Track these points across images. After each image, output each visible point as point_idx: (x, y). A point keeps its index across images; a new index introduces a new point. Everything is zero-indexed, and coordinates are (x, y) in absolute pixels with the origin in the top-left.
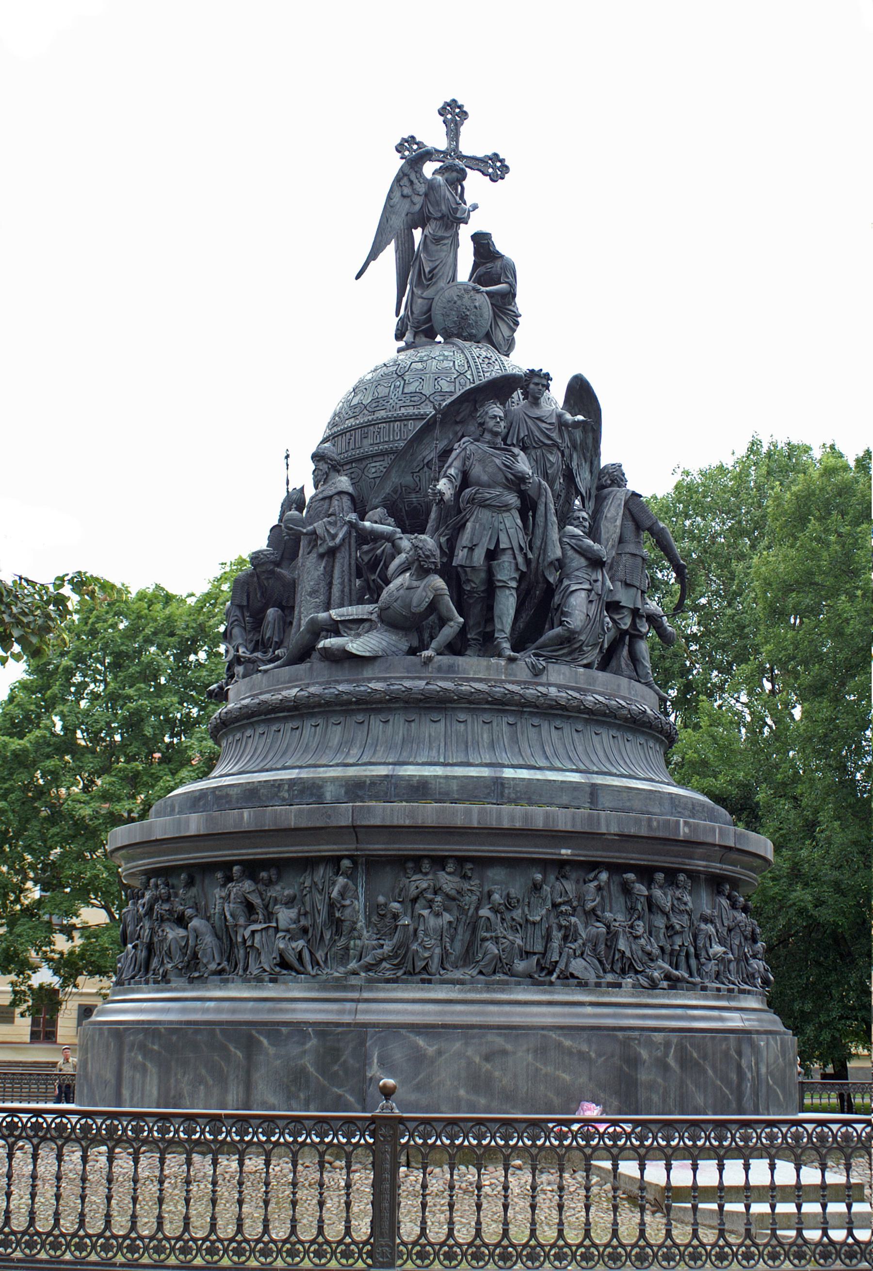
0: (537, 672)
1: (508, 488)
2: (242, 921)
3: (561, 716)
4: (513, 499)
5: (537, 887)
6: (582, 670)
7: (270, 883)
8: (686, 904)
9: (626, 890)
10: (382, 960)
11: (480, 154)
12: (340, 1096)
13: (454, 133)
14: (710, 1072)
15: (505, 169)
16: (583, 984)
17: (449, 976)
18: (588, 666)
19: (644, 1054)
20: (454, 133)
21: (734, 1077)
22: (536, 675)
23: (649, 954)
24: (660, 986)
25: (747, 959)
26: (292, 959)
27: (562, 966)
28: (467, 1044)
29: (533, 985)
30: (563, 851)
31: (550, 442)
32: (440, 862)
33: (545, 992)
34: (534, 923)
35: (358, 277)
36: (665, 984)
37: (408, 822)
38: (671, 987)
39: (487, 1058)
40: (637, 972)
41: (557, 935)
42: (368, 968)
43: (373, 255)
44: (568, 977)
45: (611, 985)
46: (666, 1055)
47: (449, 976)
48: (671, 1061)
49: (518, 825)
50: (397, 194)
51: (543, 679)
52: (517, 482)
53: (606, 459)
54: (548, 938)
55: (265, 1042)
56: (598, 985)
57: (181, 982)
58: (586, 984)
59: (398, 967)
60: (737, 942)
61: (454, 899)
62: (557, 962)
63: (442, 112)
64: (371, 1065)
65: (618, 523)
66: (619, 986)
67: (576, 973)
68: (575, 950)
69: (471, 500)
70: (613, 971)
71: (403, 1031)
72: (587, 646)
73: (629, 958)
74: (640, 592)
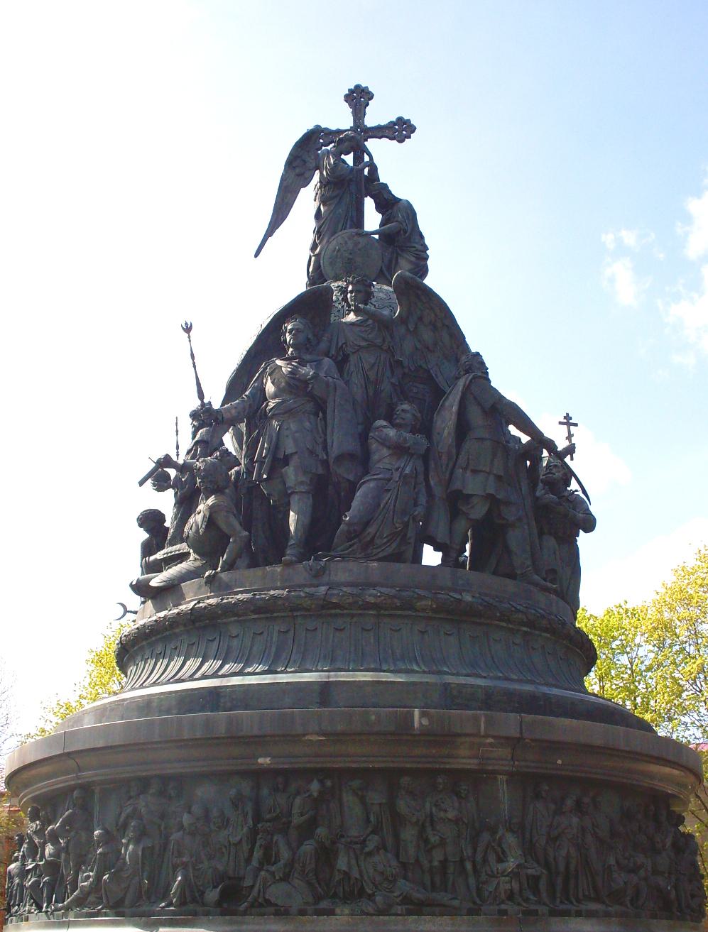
3: (342, 615)
6: (375, 564)
11: (384, 122)
13: (359, 112)
15: (412, 129)
20: (359, 112)
24: (393, 911)
27: (255, 892)
30: (260, 760)
35: (257, 255)
36: (399, 909)
38: (409, 913)
45: (320, 913)
51: (325, 579)
56: (302, 913)
65: (455, 409)
67: (273, 900)
68: (273, 874)
73: (356, 879)
74: (491, 478)
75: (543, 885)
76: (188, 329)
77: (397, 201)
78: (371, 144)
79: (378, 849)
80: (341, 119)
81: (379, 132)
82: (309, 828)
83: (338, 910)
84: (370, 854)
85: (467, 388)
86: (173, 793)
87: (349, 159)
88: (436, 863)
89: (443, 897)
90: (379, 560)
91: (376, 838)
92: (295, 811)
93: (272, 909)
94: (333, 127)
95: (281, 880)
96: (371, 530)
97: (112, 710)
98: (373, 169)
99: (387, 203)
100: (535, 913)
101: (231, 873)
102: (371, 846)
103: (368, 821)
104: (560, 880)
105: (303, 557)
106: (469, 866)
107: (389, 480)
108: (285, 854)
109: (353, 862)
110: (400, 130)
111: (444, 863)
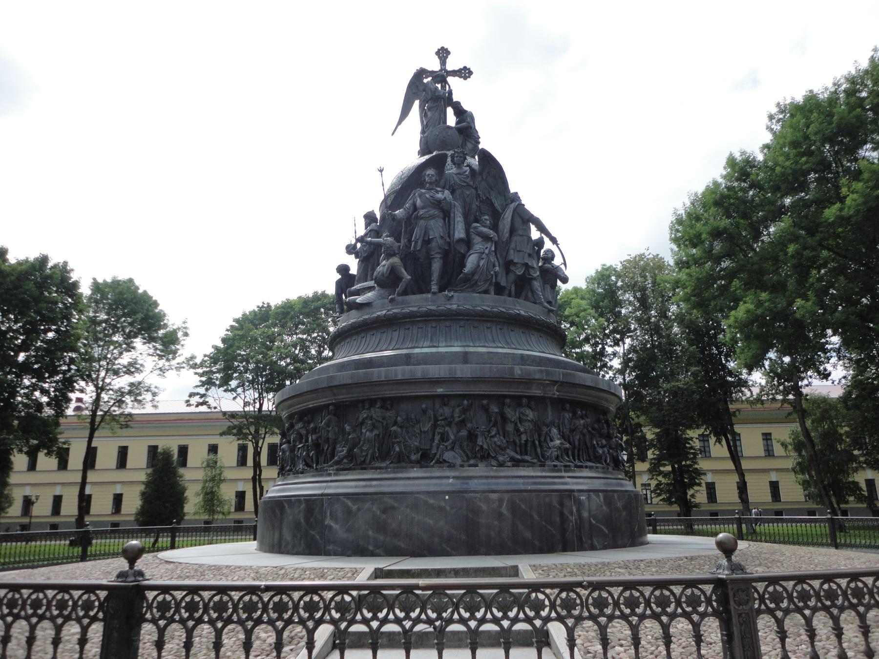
1: (435, 208)
3: (463, 320)
4: (436, 212)
6: (478, 294)
7: (309, 423)
8: (527, 416)
10: (343, 459)
11: (457, 68)
12: (313, 535)
13: (443, 62)
14: (536, 517)
15: (471, 73)
16: (451, 466)
18: (486, 292)
19: (484, 507)
20: (443, 62)
21: (558, 519)
23: (499, 446)
25: (595, 448)
26: (309, 461)
27: (438, 456)
28: (373, 504)
32: (372, 402)
33: (426, 472)
34: (425, 432)
35: (393, 134)
36: (509, 464)
38: (513, 466)
39: (384, 511)
40: (493, 458)
41: (437, 437)
42: (338, 463)
43: (400, 123)
44: (442, 462)
45: (470, 466)
46: (500, 506)
47: (377, 465)
48: (504, 510)
49: (407, 377)
53: (512, 191)
54: (433, 440)
55: (286, 506)
56: (462, 466)
59: (351, 461)
60: (578, 437)
61: (379, 422)
62: (436, 454)
63: (438, 53)
64: (326, 517)
66: (476, 466)
67: (447, 459)
70: (475, 457)
71: (341, 497)
72: (480, 282)
75: (570, 453)
76: (381, 171)
77: (465, 112)
78: (450, 79)
79: (496, 434)
80: (434, 65)
81: (454, 73)
82: (463, 422)
83: (479, 465)
84: (493, 437)
85: (515, 210)
86: (389, 407)
87: (439, 86)
88: (523, 442)
89: (527, 458)
90: (480, 293)
91: (495, 429)
92: (456, 415)
93: (447, 464)
94: (430, 69)
95: (450, 450)
96: (476, 277)
97: (348, 365)
98: (450, 93)
99: (460, 112)
100: (569, 466)
101: (423, 447)
102: (493, 433)
103: (490, 421)
104: (576, 451)
105: (441, 289)
106: (537, 443)
107: (483, 253)
108: (452, 437)
109: (484, 440)
110: (465, 73)
111: (526, 441)
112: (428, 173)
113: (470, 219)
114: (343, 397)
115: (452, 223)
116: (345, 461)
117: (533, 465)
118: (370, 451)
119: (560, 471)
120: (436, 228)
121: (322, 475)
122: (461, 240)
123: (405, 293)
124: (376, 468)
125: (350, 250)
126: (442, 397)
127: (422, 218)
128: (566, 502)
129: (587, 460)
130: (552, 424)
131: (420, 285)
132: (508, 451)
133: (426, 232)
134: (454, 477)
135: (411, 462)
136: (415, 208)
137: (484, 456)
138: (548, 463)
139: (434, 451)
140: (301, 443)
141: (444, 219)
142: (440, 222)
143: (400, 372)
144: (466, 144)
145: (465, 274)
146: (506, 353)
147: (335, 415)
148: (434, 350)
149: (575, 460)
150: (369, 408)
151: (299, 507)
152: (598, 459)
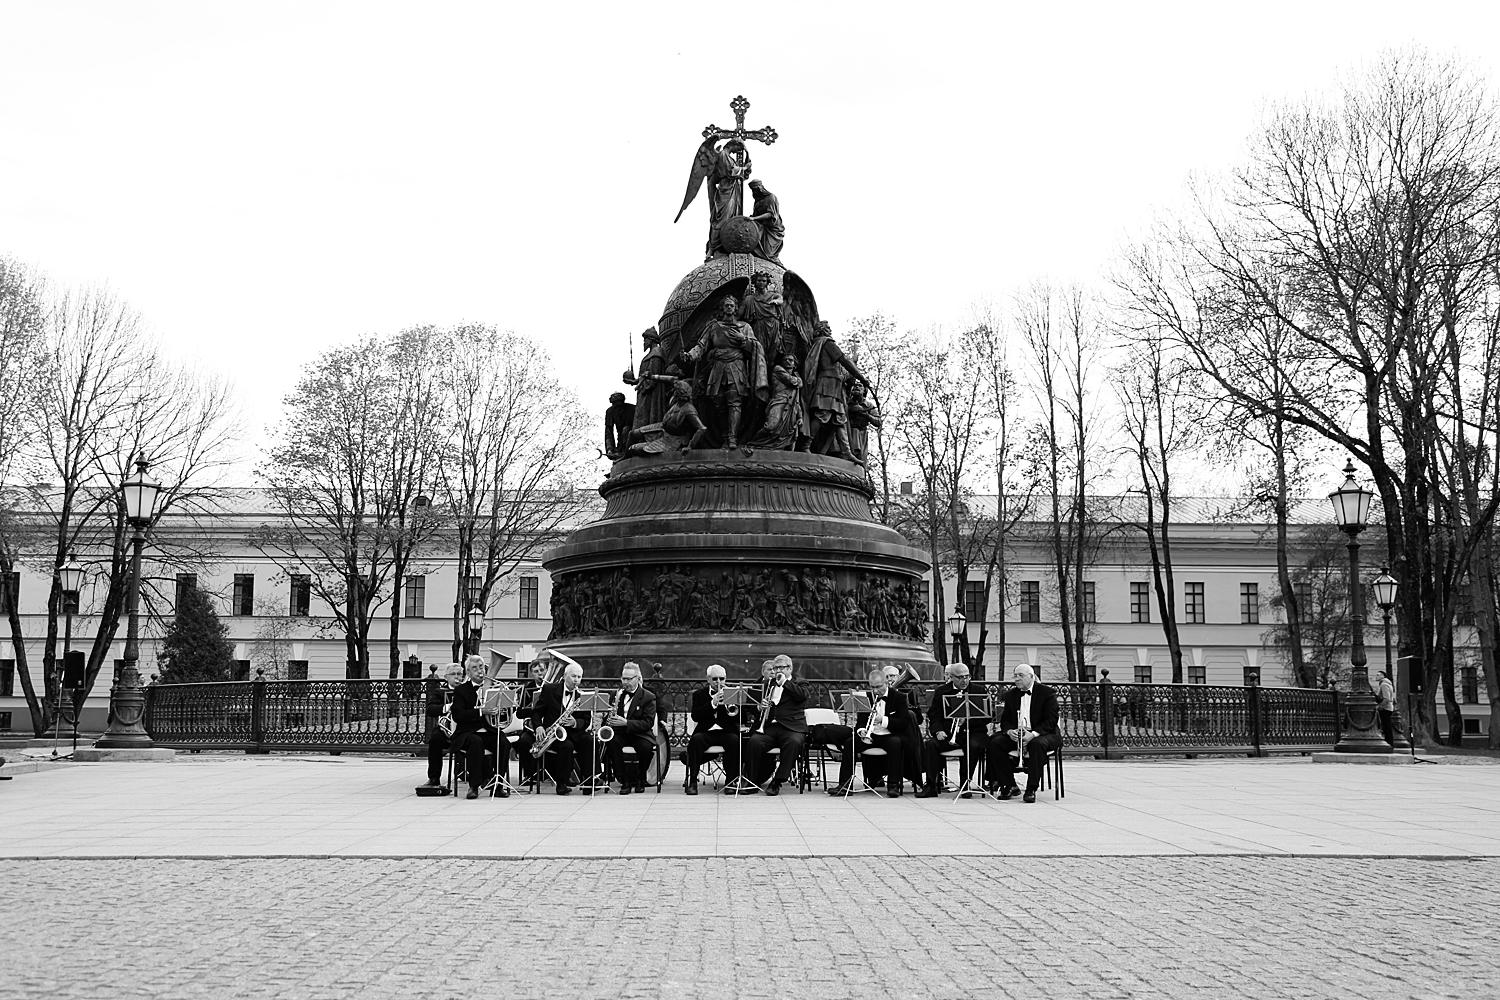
0: (749, 455)
1: (734, 348)
2: (583, 604)
4: (736, 354)
5: (725, 579)
7: (595, 582)
8: (825, 585)
9: (784, 578)
13: (740, 119)
15: (775, 135)
16: (750, 632)
17: (677, 629)
18: (788, 448)
20: (740, 119)
22: (748, 457)
23: (796, 614)
29: (721, 633)
31: (768, 315)
32: (671, 567)
37: (650, 546)
38: (809, 634)
41: (737, 605)
42: (633, 626)
43: (685, 206)
44: (741, 629)
47: (677, 629)
50: (698, 165)
52: (738, 344)
54: (732, 607)
56: (760, 632)
57: (559, 638)
58: (753, 632)
60: (875, 607)
61: (679, 587)
63: (733, 105)
65: (817, 359)
69: (713, 356)
70: (773, 625)
71: (644, 659)
75: (866, 622)
78: (749, 144)
80: (730, 124)
81: (756, 135)
84: (791, 605)
87: (734, 156)
89: (823, 626)
91: (793, 598)
102: (791, 602)
103: (789, 589)
110: (767, 136)
111: (823, 610)
112: (726, 303)
113: (775, 359)
114: (640, 560)
115: (753, 367)
116: (643, 624)
117: (827, 633)
118: (670, 615)
119: (854, 639)
120: (736, 372)
121: (618, 638)
122: (763, 388)
123: (698, 446)
124: (672, 633)
125: (628, 378)
126: (742, 565)
127: (719, 360)
128: (857, 667)
129: (883, 630)
130: (850, 593)
131: (715, 439)
132: (805, 619)
133: (725, 378)
134: (752, 643)
135: (711, 627)
136: (711, 344)
137: (782, 624)
138: (842, 632)
139: (734, 618)
140: (587, 604)
141: (744, 360)
142: (740, 364)
143: (703, 538)
144: (767, 239)
145: (769, 430)
146: (807, 521)
147: (629, 577)
148: (734, 515)
149: (870, 629)
150: (669, 572)
151: (598, 667)
152: (895, 629)
